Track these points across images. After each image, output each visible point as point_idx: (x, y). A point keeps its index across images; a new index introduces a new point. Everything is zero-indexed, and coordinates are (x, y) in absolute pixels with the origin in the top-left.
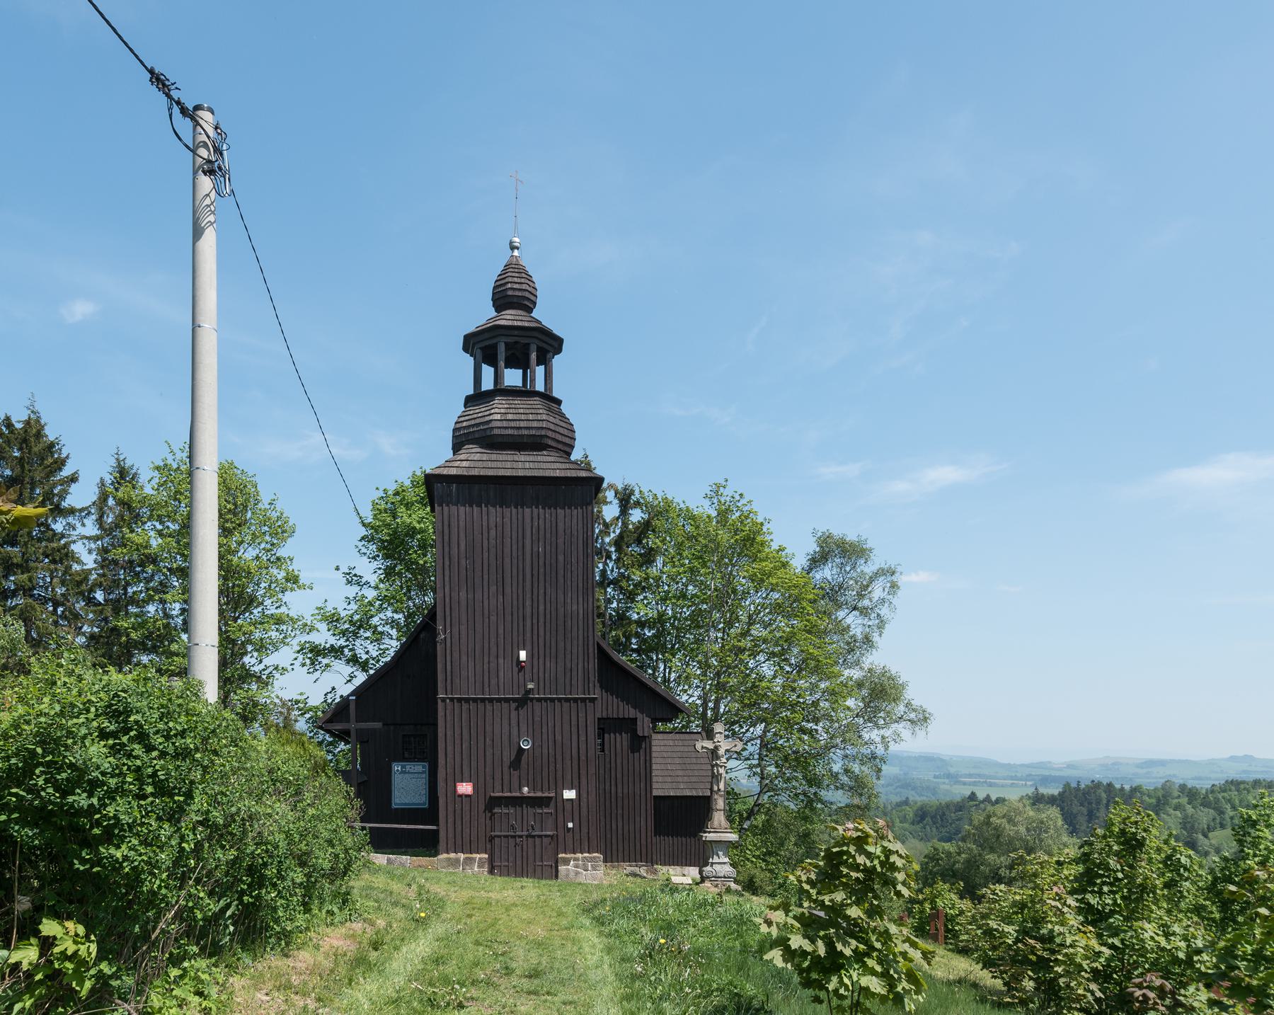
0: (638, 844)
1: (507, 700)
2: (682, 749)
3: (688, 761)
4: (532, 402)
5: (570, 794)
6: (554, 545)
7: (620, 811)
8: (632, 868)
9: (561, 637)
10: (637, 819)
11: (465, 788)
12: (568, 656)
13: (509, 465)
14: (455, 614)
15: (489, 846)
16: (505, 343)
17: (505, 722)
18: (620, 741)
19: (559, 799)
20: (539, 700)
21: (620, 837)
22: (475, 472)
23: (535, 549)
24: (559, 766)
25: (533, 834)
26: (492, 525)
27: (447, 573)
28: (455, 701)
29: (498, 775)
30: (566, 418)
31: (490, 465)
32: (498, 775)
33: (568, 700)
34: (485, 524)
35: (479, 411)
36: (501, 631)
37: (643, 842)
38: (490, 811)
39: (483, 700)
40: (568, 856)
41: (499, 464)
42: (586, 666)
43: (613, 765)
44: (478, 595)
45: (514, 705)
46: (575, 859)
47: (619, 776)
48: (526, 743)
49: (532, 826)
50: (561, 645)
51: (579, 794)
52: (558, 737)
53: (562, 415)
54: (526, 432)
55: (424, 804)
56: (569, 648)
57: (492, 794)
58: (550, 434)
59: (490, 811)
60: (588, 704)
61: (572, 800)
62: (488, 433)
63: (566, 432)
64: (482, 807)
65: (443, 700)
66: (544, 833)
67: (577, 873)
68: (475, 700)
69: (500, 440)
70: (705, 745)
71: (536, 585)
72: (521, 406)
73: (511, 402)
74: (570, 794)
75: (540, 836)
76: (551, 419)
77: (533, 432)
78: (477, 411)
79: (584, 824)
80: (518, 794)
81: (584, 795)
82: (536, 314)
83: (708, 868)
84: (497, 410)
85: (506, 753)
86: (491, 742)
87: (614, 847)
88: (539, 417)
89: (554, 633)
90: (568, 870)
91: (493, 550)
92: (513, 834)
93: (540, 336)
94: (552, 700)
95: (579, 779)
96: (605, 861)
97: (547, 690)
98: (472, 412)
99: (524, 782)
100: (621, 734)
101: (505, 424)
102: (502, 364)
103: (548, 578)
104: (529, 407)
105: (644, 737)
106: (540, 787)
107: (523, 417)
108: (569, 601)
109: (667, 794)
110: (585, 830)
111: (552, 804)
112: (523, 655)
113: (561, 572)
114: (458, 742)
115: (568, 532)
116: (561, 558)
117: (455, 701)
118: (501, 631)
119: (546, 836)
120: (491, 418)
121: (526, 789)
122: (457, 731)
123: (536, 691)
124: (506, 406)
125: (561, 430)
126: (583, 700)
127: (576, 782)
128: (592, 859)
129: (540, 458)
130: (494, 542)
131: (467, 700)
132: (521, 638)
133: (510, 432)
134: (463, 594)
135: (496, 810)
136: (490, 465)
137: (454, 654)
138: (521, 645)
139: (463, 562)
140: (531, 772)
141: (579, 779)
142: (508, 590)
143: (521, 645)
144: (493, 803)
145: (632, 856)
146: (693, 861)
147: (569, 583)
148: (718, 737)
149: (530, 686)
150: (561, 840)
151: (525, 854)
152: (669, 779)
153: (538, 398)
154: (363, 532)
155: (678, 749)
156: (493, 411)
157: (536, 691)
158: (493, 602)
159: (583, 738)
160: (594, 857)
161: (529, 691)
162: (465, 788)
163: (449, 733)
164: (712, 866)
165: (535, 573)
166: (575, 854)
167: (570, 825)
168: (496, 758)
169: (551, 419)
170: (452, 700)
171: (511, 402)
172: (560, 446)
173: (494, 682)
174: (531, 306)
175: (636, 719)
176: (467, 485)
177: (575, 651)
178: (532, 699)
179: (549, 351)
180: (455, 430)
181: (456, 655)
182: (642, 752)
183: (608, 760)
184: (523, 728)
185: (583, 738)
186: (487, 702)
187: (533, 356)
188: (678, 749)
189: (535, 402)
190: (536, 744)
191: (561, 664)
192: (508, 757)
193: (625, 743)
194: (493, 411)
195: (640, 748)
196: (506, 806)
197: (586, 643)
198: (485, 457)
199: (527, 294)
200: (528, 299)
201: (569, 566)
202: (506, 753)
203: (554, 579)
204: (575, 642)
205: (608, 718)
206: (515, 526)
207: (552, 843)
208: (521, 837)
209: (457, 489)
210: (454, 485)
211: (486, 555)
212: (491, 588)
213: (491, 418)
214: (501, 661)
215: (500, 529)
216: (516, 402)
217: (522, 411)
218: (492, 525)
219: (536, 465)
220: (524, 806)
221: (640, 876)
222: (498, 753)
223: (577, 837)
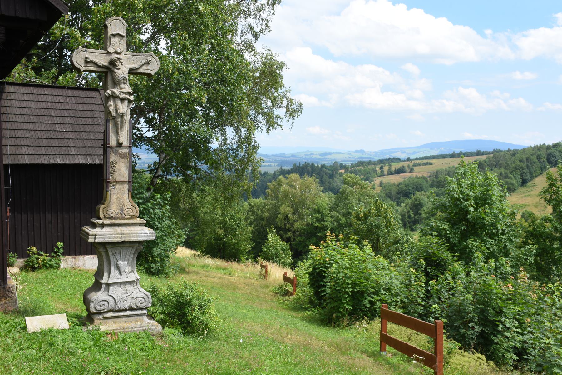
2: (75, 107)
109: (52, 162)
152: (56, 143)
155: (70, 106)
188: (70, 106)
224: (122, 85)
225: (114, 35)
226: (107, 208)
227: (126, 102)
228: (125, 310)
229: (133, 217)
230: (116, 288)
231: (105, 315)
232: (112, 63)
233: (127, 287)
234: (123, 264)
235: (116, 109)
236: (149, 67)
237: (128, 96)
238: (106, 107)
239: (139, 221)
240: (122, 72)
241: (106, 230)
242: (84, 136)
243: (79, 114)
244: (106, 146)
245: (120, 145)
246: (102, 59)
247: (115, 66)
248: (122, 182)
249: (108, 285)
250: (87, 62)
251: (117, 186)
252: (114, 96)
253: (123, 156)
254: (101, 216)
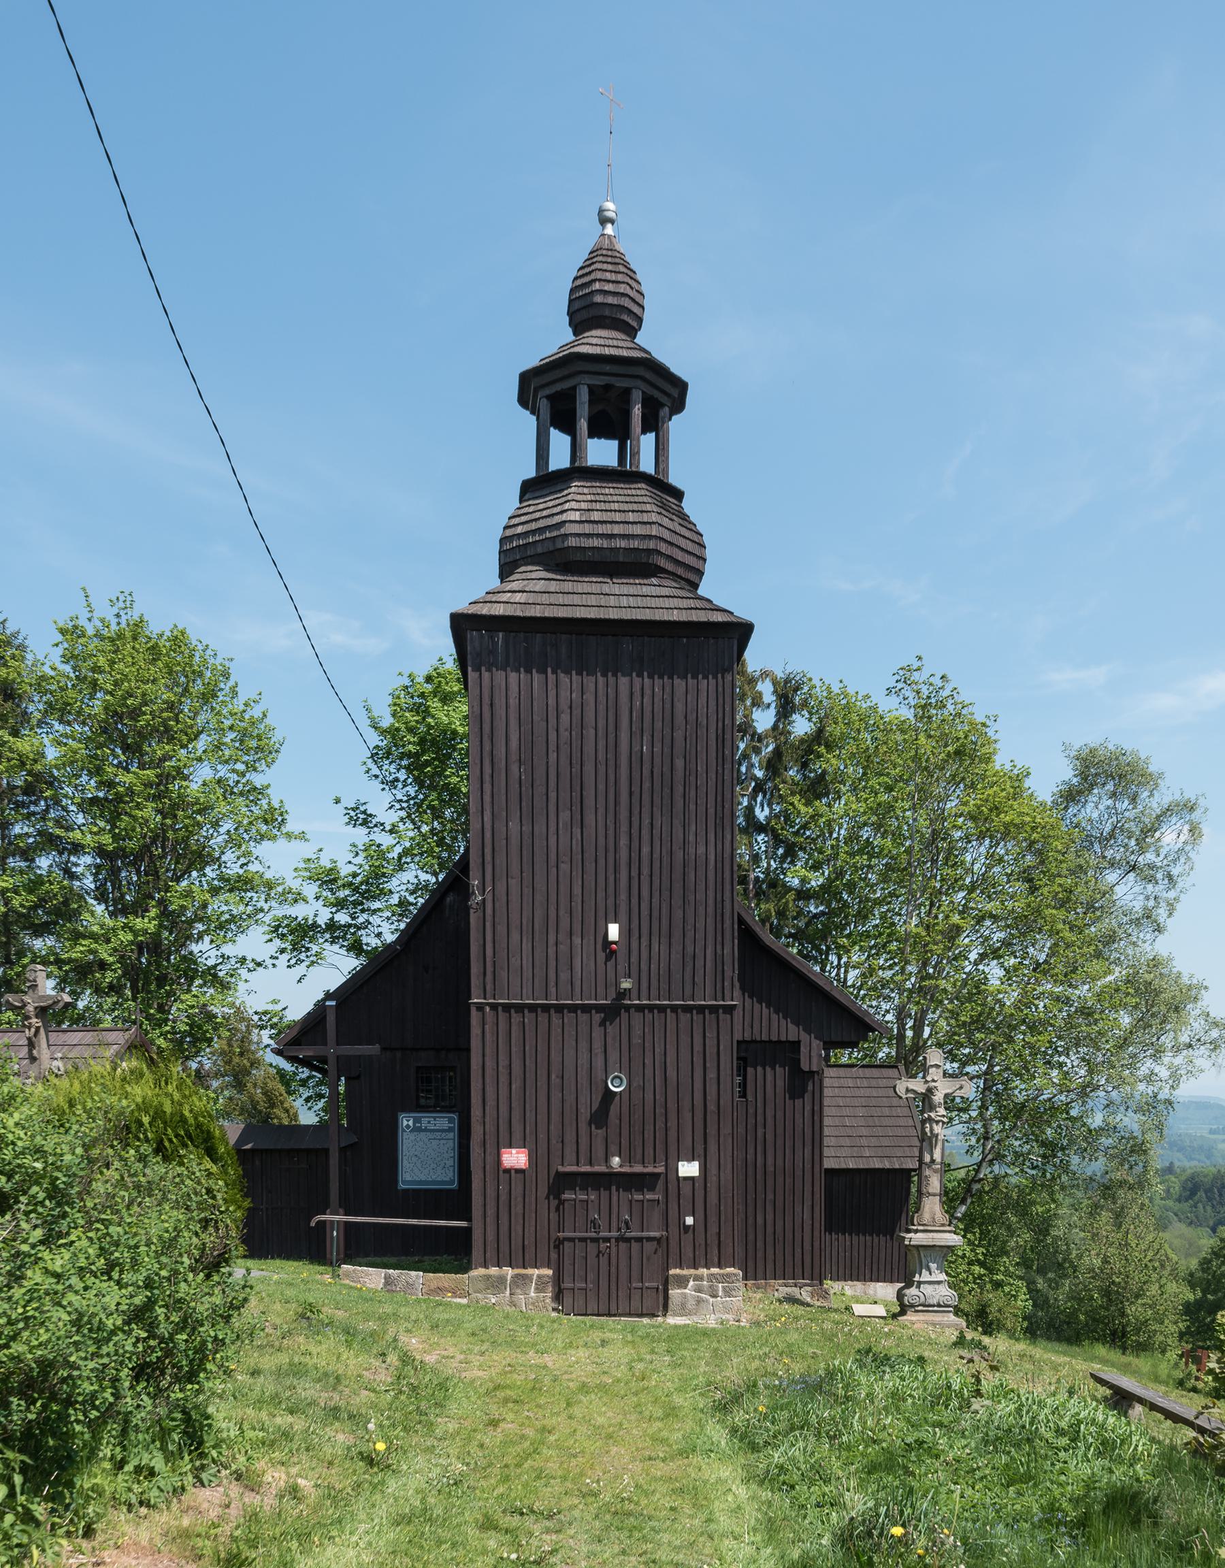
0: (798, 1251)
1: (586, 1009)
2: (868, 1092)
3: (874, 1112)
4: (634, 492)
5: (689, 1169)
6: (667, 741)
7: (770, 1196)
8: (789, 1290)
9: (677, 901)
10: (798, 1209)
11: (515, 1158)
12: (690, 934)
13: (592, 600)
14: (501, 860)
15: (554, 1256)
16: (589, 386)
17: (584, 1045)
18: (774, 1078)
19: (671, 1177)
20: (640, 1008)
21: (770, 1239)
22: (536, 612)
23: (636, 748)
24: (672, 1123)
25: (628, 1235)
26: (564, 705)
27: (487, 787)
28: (500, 1008)
29: (570, 1137)
30: (690, 523)
31: (561, 599)
32: (570, 1137)
33: (688, 1009)
34: (552, 701)
35: (543, 505)
36: (577, 890)
37: (807, 1247)
38: (557, 1197)
39: (546, 1008)
40: (685, 1272)
41: (576, 599)
42: (719, 951)
43: (760, 1118)
44: (540, 828)
45: (597, 1017)
46: (698, 1278)
47: (770, 1137)
48: (617, 1082)
49: (627, 1223)
50: (678, 914)
51: (704, 1169)
52: (672, 1073)
53: (684, 517)
54: (622, 544)
55: (452, 1182)
56: (691, 920)
57: (561, 1169)
58: (663, 547)
59: (557, 1197)
60: (722, 1016)
61: (692, 1179)
62: (559, 545)
63: (690, 546)
64: (543, 1190)
65: (480, 1007)
66: (645, 1234)
68: (533, 1008)
69: (579, 557)
71: (636, 811)
72: (615, 498)
73: (599, 491)
74: (689, 1169)
75: (639, 1240)
76: (666, 522)
77: (635, 544)
78: (541, 507)
79: (713, 1219)
80: (603, 1169)
81: (713, 1170)
82: (640, 339)
83: (913, 1291)
84: (573, 505)
85: (584, 1099)
86: (559, 1081)
87: (760, 1254)
88: (645, 518)
89: (666, 894)
90: (685, 1296)
91: (565, 749)
92: (594, 1235)
93: (649, 375)
94: (662, 1009)
95: (705, 1143)
96: (746, 1278)
97: (654, 992)
98: (531, 509)
99: (613, 1148)
100: (774, 1068)
101: (587, 529)
102: (583, 425)
103: (657, 800)
104: (628, 499)
105: (812, 1073)
106: (639, 1156)
107: (618, 517)
108: (692, 838)
109: (843, 1166)
110: (713, 1229)
111: (660, 1184)
112: (614, 931)
113: (679, 789)
114: (503, 1079)
115: (692, 717)
116: (679, 763)
117: (500, 1008)
118: (577, 890)
119: (649, 1239)
120: (564, 517)
121: (616, 1160)
122: (503, 1062)
123: (634, 993)
124: (589, 497)
125: (683, 543)
126: (714, 1009)
127: (699, 1149)
128: (725, 1278)
129: (646, 590)
130: (567, 734)
131: (520, 1008)
132: (611, 901)
133: (596, 543)
134: (514, 826)
135: (567, 1195)
136: (561, 599)
137: (499, 928)
138: (611, 915)
139: (514, 768)
140: (625, 1133)
141: (705, 1143)
142: (590, 818)
143: (611, 915)
144: (562, 1182)
145: (789, 1270)
146: (882, 1273)
147: (692, 807)
149: (626, 984)
150: (673, 1243)
151: (613, 1270)
152: (847, 1142)
153: (643, 486)
154: (374, 739)
155: (862, 1092)
156: (567, 506)
157: (634, 993)
158: (564, 840)
159: (712, 1075)
160: (728, 1275)
161: (623, 994)
162: (515, 1158)
163: (489, 1064)
164: (918, 1287)
165: (636, 789)
166: (695, 1268)
167: (689, 1221)
168: (567, 1106)
169: (666, 522)
170: (494, 1007)
171: (599, 491)
172: (680, 571)
173: (564, 976)
174: (635, 324)
175: (799, 1042)
176: (522, 635)
177: (700, 925)
178: (628, 1008)
179: (662, 405)
180: (503, 540)
181: (502, 929)
182: (807, 1096)
183: (751, 1111)
184: (613, 1056)
185: (712, 1075)
186: (552, 1011)
187: (637, 411)
188: (862, 1092)
189: (639, 492)
190: (635, 1084)
191: (677, 948)
192: (588, 1104)
193: (780, 1083)
194: (567, 506)
195: (804, 1090)
196: (584, 1188)
197: (719, 911)
198: (553, 586)
199: (626, 303)
200: (630, 312)
201: (693, 778)
202: (584, 1099)
203: (667, 801)
204: (701, 910)
205: (753, 1041)
206: (602, 708)
207: (660, 1252)
208: (607, 1240)
209: (506, 641)
210: (501, 635)
211: (553, 756)
212: (561, 814)
213: (564, 517)
214: (577, 941)
215: (577, 712)
216: (607, 491)
217: (616, 506)
218: (564, 705)
219: (640, 602)
220: (614, 1188)
221: (803, 1304)
222: (570, 1099)
223: (700, 1240)
226: (920, 1217)
228: (933, 1306)
229: (943, 1225)
230: (926, 1286)
232: (930, 1091)
234: (933, 1266)
238: (923, 1129)
239: (948, 1228)
240: (938, 1097)
241: (919, 1235)
242: (880, 1132)
243: (873, 1102)
244: (921, 1161)
245: (933, 1161)
246: (918, 1085)
247: (932, 1093)
248: (934, 1195)
249: (920, 1283)
250: (908, 1090)
252: (930, 1119)
253: (935, 1171)
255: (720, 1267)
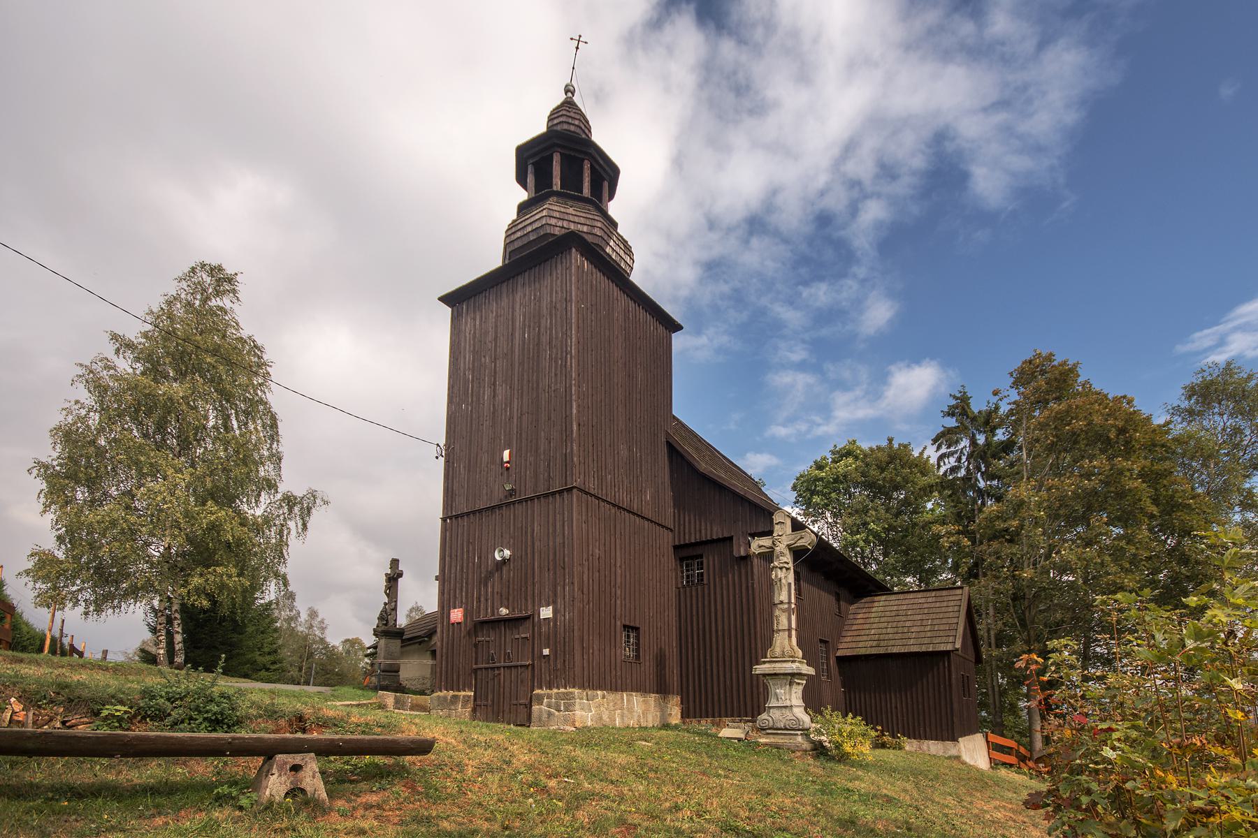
46: (549, 697)
51: (555, 612)
67: (550, 714)
70: (761, 543)
128: (568, 697)
148: (777, 530)
164: (769, 712)
166: (551, 689)
224: (781, 558)
225: (777, 524)
227: (784, 569)
231: (768, 731)
233: (784, 710)
235: (776, 576)
236: (803, 540)
237: (786, 565)
249: (770, 708)
251: (781, 633)
253: (784, 611)
254: (768, 656)
255: (566, 688)
